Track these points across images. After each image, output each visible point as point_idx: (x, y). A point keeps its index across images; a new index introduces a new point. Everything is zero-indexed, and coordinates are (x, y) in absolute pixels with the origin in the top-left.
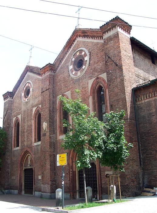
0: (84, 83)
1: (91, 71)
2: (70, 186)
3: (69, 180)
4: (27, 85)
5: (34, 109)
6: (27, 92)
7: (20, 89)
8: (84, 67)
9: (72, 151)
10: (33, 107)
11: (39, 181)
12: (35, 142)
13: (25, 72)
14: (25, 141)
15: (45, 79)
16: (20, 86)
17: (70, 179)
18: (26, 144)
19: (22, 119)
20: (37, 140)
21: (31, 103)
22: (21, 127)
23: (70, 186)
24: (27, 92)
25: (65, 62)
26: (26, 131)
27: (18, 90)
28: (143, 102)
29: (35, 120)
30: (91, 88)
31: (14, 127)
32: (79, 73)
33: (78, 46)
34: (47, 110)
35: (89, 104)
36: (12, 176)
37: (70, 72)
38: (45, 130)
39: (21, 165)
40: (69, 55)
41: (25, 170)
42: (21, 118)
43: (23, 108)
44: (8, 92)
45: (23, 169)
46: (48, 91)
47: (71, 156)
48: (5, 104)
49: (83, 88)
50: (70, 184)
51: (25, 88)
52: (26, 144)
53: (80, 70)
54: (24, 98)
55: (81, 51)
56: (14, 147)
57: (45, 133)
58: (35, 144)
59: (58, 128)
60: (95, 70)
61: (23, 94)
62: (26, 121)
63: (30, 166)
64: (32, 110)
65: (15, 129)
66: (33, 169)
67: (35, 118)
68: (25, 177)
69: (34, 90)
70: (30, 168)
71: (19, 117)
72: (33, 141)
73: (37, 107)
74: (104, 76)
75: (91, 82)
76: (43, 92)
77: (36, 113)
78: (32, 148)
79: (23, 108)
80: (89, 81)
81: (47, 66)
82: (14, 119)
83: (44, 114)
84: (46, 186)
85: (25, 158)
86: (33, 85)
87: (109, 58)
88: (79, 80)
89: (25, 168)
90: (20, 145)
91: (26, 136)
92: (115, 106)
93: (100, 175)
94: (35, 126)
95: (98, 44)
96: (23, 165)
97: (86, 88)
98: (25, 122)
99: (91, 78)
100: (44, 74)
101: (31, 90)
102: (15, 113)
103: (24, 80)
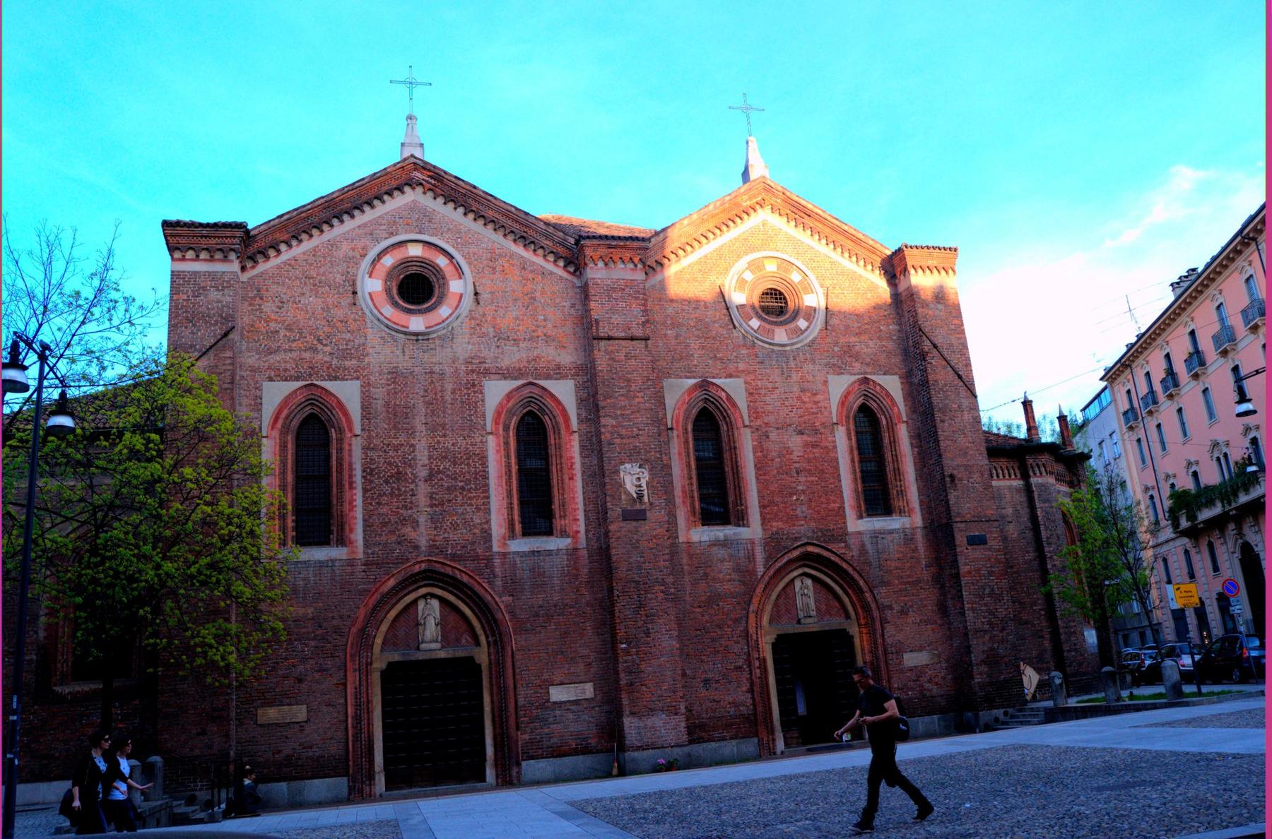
0: (810, 378)
1: (836, 349)
2: (755, 709)
3: (751, 691)
4: (415, 251)
5: (495, 392)
6: (417, 287)
7: (333, 244)
8: (802, 323)
9: (759, 590)
10: (487, 373)
11: (558, 713)
12: (512, 535)
13: (394, 184)
14: (415, 524)
15: (614, 290)
16: (330, 234)
17: (752, 684)
18: (422, 536)
19: (379, 405)
20: (518, 527)
21: (463, 347)
22: (366, 449)
23: (755, 709)
24: (417, 287)
25: (699, 262)
26: (423, 473)
27: (307, 245)
28: (994, 483)
29: (507, 437)
30: (842, 403)
31: (276, 434)
32: (780, 336)
33: (767, 237)
34: (642, 419)
35: (835, 447)
36: (270, 704)
37: (735, 313)
38: (640, 496)
39: (364, 640)
40: (721, 247)
41: (392, 674)
42: (366, 407)
43: (382, 355)
44: (240, 226)
45: (379, 665)
46: (641, 344)
47: (753, 607)
48: (178, 281)
49: (803, 391)
50: (754, 705)
51: (388, 261)
52: (422, 536)
53: (788, 327)
54: (388, 311)
55: (786, 264)
56: (283, 543)
57: (638, 507)
58: (521, 545)
59: (678, 501)
60: (848, 351)
61: (373, 285)
62: (420, 427)
63: (443, 647)
64: (474, 388)
65: (283, 446)
66: (482, 656)
67: (506, 428)
68: (385, 704)
69: (484, 296)
70: (442, 655)
71: (348, 393)
72: (497, 526)
73: (524, 385)
74: (893, 385)
75: (839, 385)
76: (610, 338)
77: (510, 404)
78: (489, 560)
79: (382, 355)
80: (829, 377)
81: (636, 244)
82: (275, 394)
83: (623, 432)
84: (658, 721)
85: (394, 605)
86: (478, 272)
87: (935, 346)
88: (781, 354)
89: (396, 657)
90: (358, 535)
91: (422, 499)
92: (961, 480)
93: (887, 663)
94: (508, 466)
95: (854, 277)
96: (379, 641)
97: (819, 398)
98: (411, 432)
99: (839, 370)
100: (601, 264)
101: (455, 286)
102: (288, 356)
103: (369, 215)
